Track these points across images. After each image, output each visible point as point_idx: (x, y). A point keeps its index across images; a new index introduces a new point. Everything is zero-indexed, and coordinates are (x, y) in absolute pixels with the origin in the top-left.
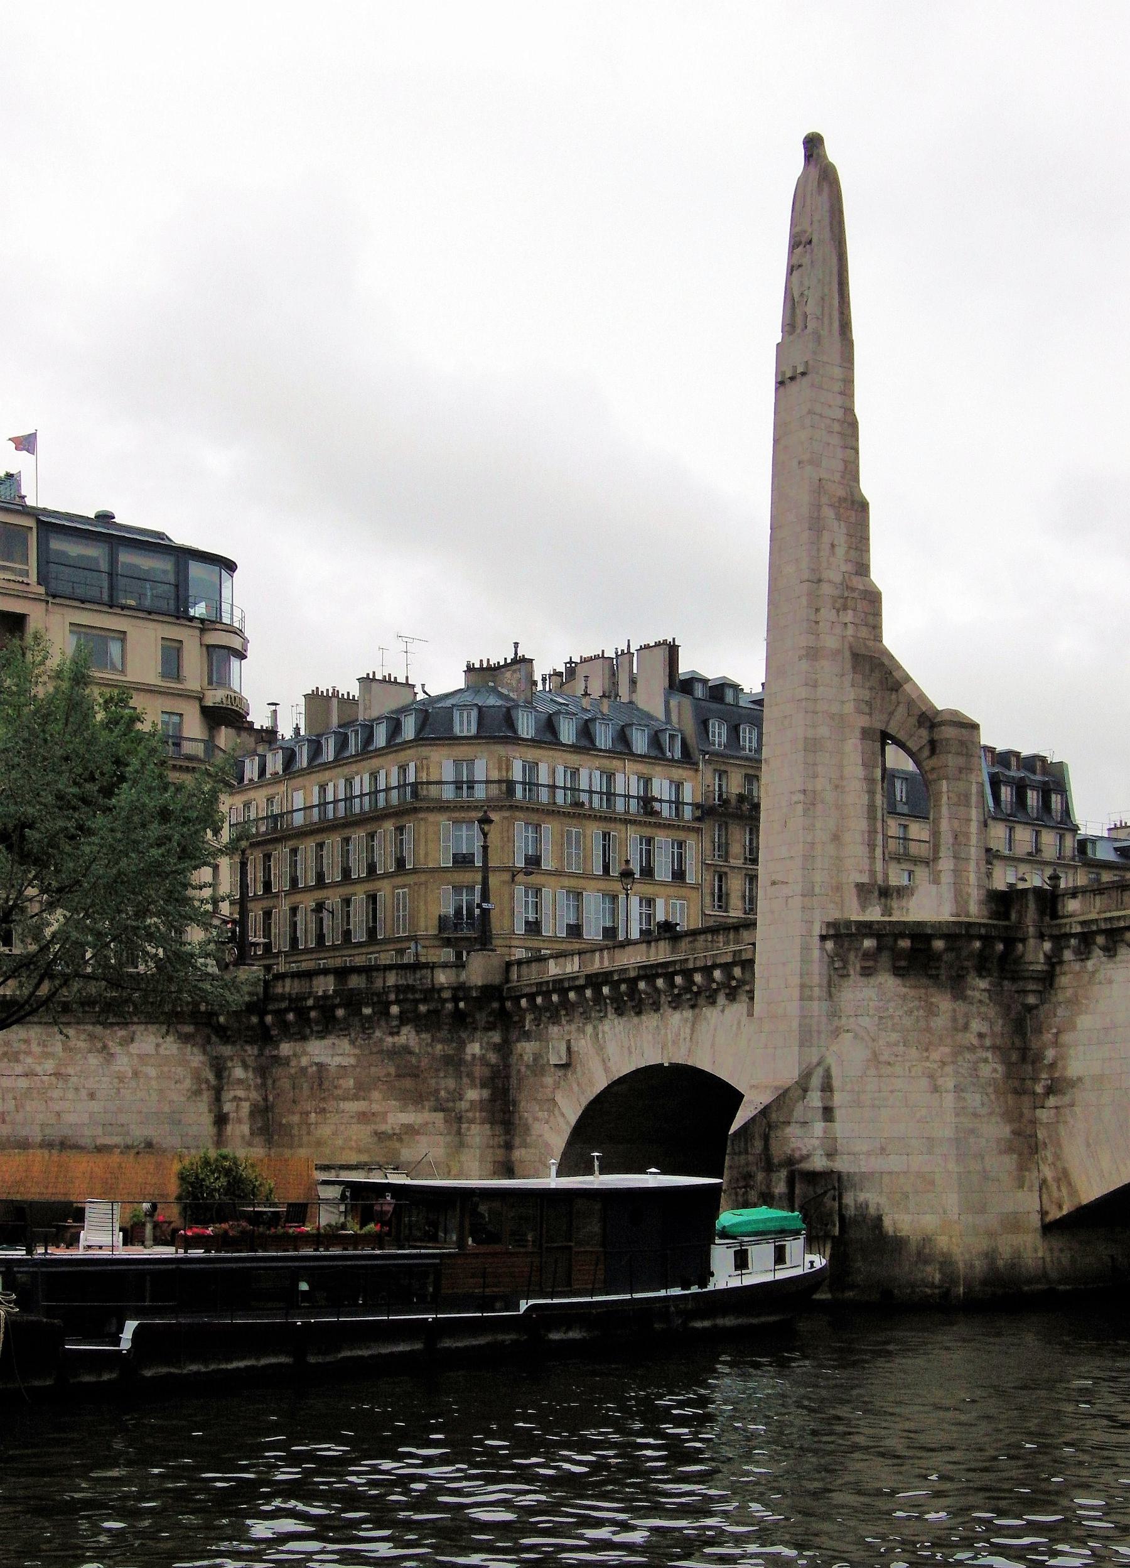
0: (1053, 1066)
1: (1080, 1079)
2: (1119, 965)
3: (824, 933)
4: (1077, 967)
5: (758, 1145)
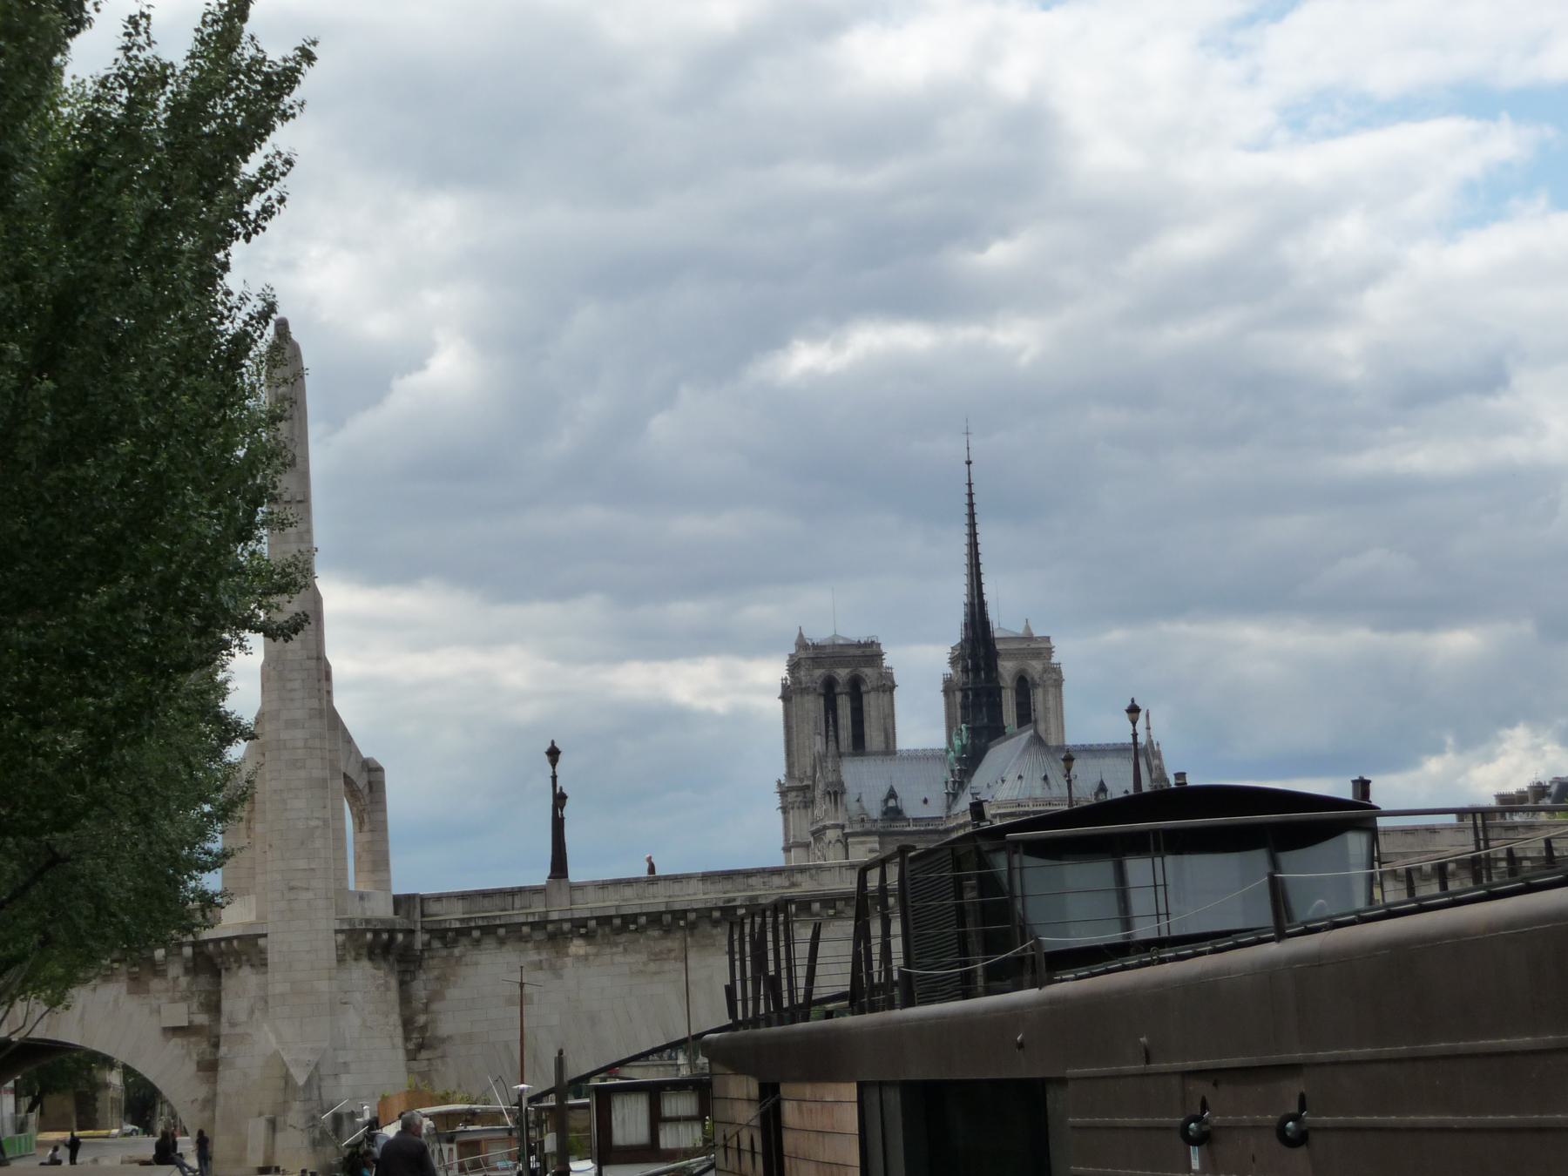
0: (424, 1028)
1: (450, 1037)
2: (484, 952)
3: (338, 928)
4: (444, 953)
5: (316, 1092)
